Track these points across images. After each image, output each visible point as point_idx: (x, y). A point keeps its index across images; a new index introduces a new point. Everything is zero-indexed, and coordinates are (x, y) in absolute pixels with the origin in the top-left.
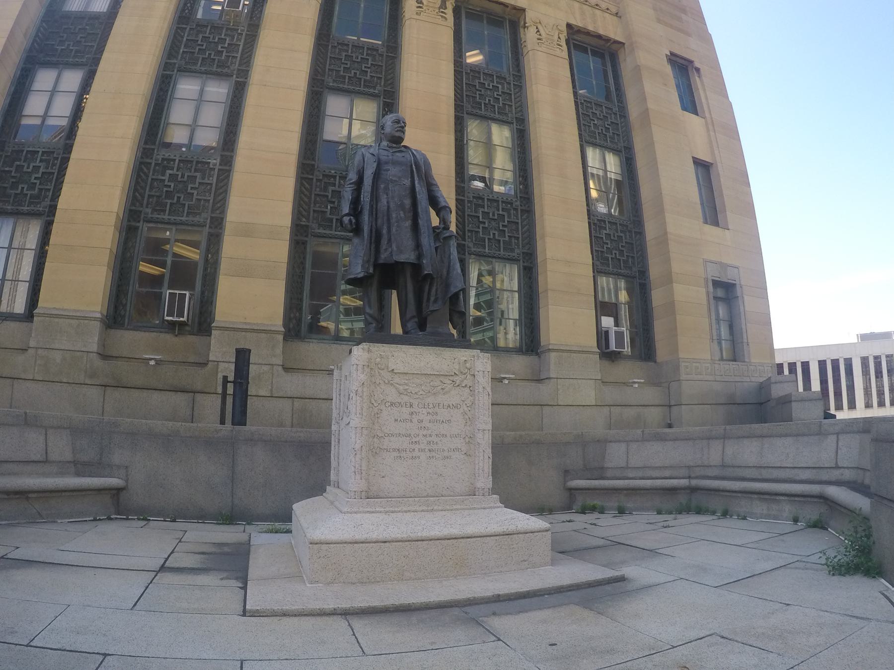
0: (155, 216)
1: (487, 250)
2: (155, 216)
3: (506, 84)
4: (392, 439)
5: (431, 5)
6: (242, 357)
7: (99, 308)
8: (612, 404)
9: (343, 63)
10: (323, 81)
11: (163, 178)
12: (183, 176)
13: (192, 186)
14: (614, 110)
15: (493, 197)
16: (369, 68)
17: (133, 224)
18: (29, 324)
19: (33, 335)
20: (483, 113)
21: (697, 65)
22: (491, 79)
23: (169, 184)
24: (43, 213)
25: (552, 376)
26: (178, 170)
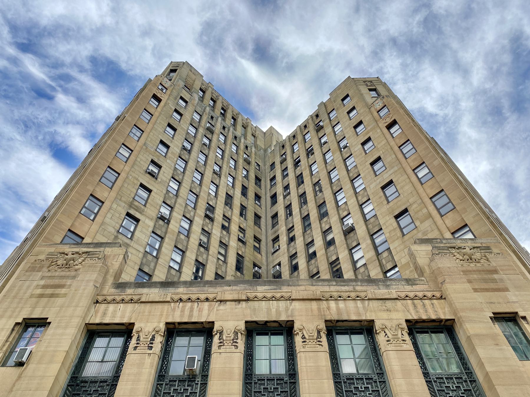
3: (373, 383)
5: (311, 337)
14: (464, 378)
21: (521, 314)
22: (362, 382)
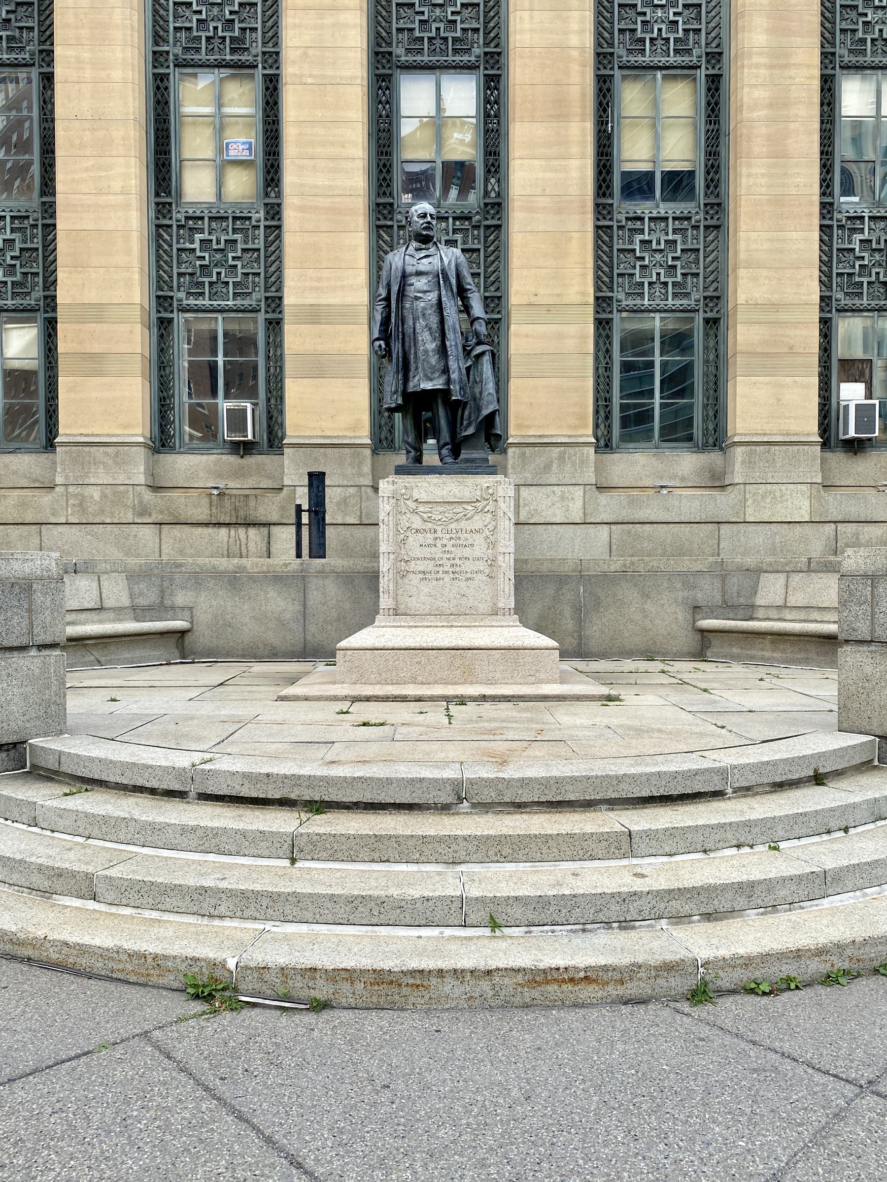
0: (192, 302)
1: (646, 302)
2: (192, 302)
4: (418, 562)
6: (317, 480)
7: (139, 431)
8: (839, 518)
9: (418, 13)
10: (390, 53)
11: (192, 246)
12: (218, 242)
13: (234, 255)
15: (659, 213)
16: (458, 13)
17: (164, 315)
18: (51, 456)
19: (58, 470)
20: (647, 59)
23: (202, 254)
24: (37, 308)
25: (736, 481)
26: (210, 233)
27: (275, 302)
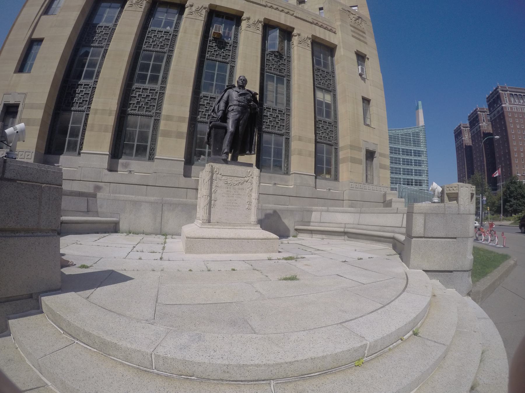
13: (148, 99)
26: (142, 93)
27: (159, 114)
